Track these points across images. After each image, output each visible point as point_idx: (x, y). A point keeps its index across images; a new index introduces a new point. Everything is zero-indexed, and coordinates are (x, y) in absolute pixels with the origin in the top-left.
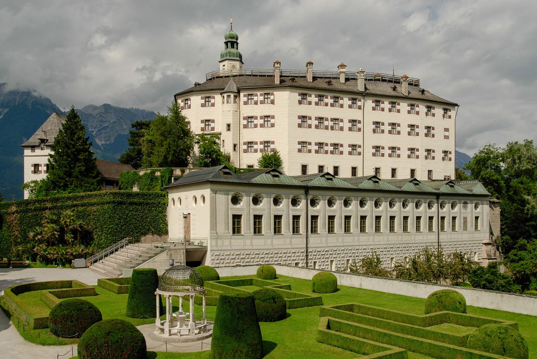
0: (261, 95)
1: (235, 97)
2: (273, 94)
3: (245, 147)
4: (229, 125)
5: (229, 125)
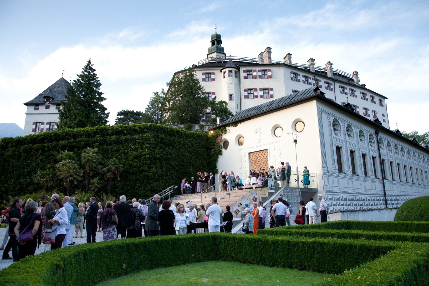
0: (259, 71)
1: (236, 72)
5: (231, 96)
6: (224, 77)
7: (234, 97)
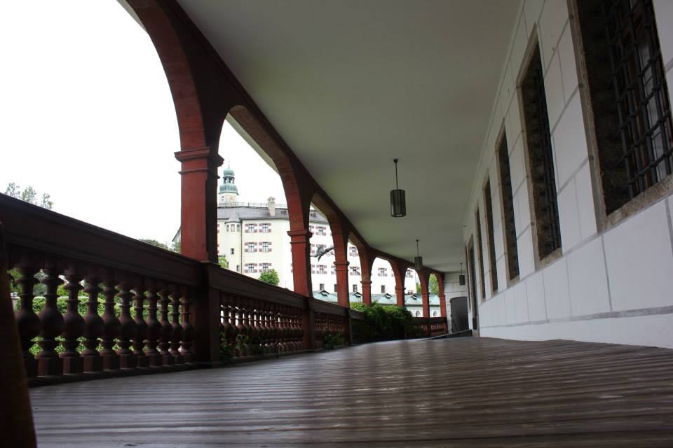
0: (260, 225)
1: (238, 226)
2: (270, 225)
3: (247, 268)
4: (233, 250)
5: (233, 250)
6: (228, 230)
7: (235, 252)
